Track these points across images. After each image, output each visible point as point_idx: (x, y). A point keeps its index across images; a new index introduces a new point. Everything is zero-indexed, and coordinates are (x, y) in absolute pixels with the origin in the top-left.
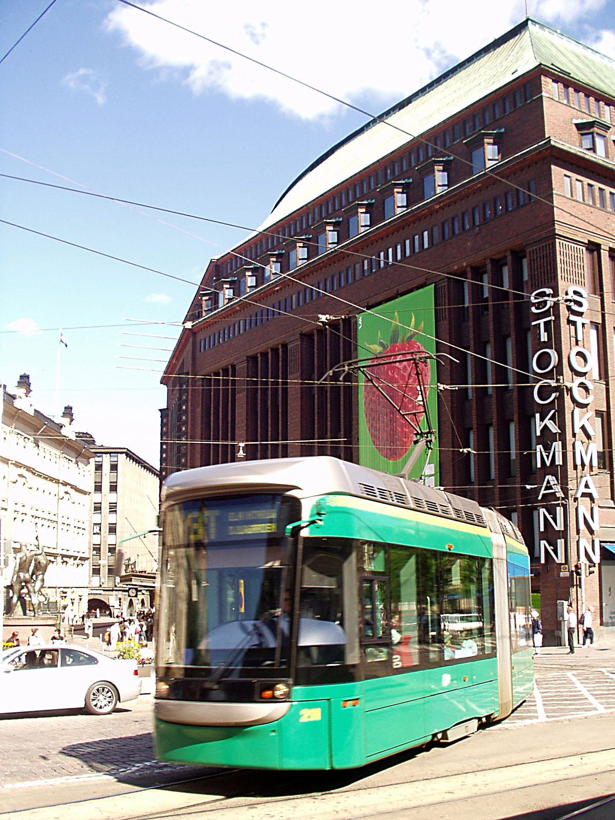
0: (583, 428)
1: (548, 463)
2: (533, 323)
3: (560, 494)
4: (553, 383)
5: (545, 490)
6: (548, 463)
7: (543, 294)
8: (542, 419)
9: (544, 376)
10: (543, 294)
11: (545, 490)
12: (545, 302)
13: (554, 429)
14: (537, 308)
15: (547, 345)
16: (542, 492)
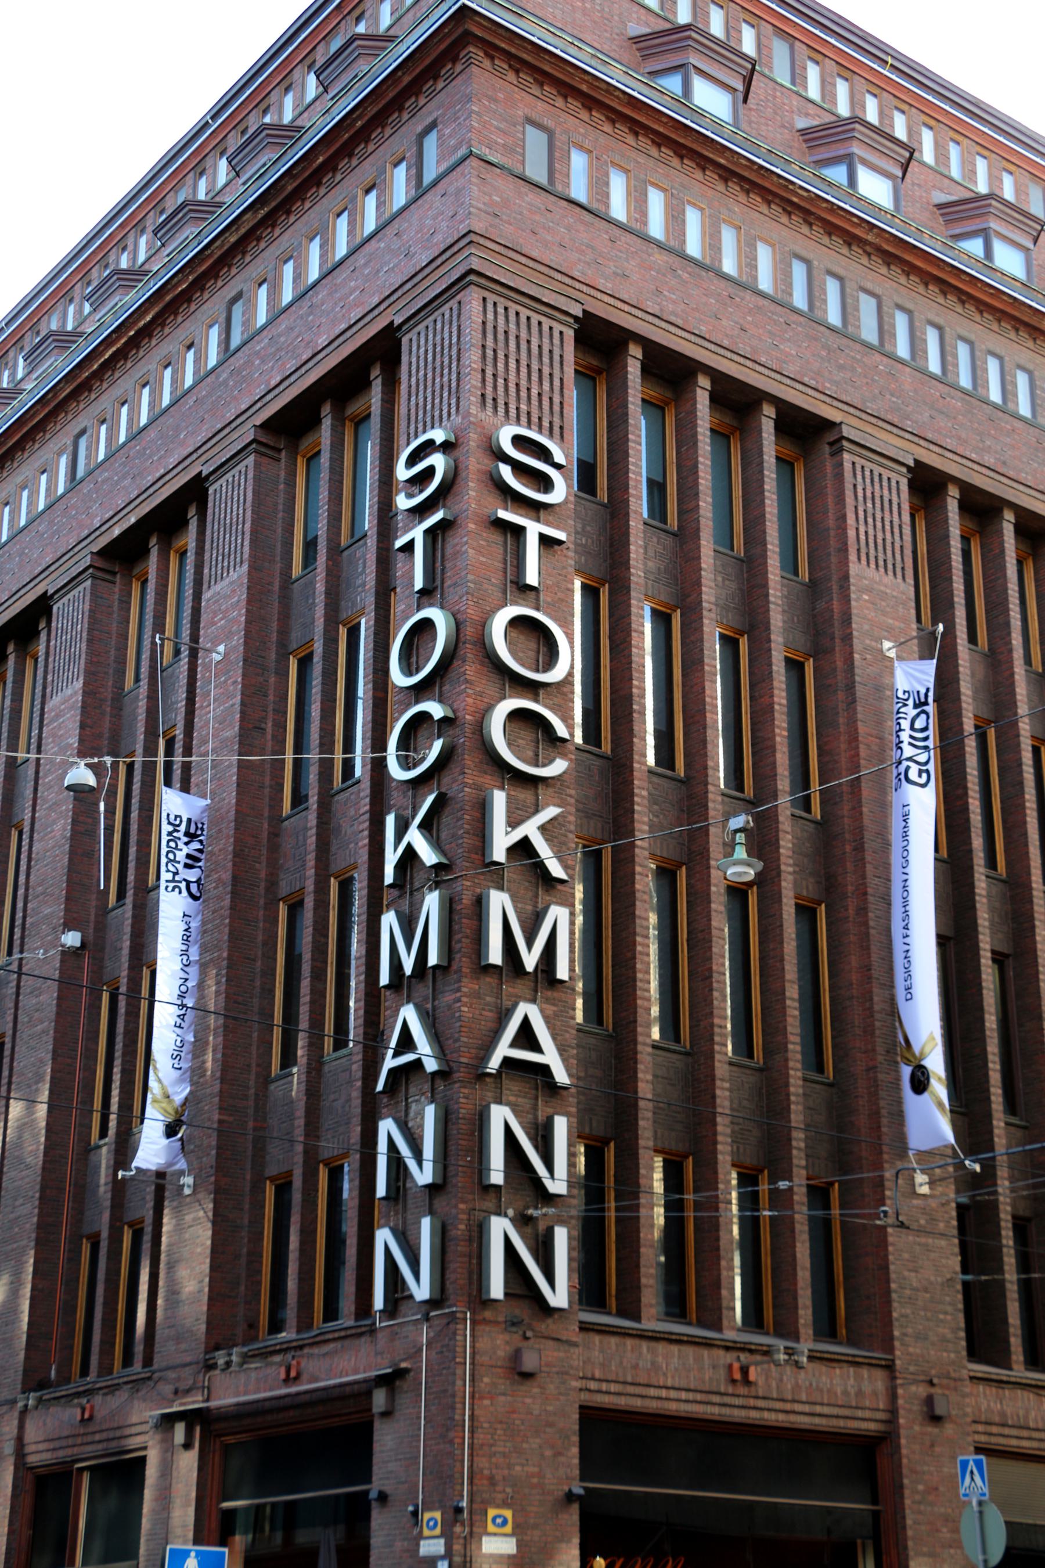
0: (523, 848)
1: (408, 965)
2: (399, 543)
3: (431, 1065)
4: (436, 710)
5: (397, 1054)
6: (408, 965)
7: (428, 447)
8: (402, 830)
9: (420, 691)
10: (428, 447)
11: (396, 1055)
12: (430, 471)
13: (428, 855)
14: (410, 496)
15: (426, 594)
16: (390, 1062)
